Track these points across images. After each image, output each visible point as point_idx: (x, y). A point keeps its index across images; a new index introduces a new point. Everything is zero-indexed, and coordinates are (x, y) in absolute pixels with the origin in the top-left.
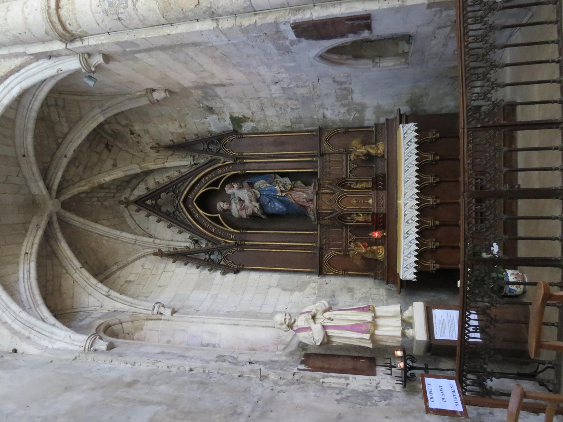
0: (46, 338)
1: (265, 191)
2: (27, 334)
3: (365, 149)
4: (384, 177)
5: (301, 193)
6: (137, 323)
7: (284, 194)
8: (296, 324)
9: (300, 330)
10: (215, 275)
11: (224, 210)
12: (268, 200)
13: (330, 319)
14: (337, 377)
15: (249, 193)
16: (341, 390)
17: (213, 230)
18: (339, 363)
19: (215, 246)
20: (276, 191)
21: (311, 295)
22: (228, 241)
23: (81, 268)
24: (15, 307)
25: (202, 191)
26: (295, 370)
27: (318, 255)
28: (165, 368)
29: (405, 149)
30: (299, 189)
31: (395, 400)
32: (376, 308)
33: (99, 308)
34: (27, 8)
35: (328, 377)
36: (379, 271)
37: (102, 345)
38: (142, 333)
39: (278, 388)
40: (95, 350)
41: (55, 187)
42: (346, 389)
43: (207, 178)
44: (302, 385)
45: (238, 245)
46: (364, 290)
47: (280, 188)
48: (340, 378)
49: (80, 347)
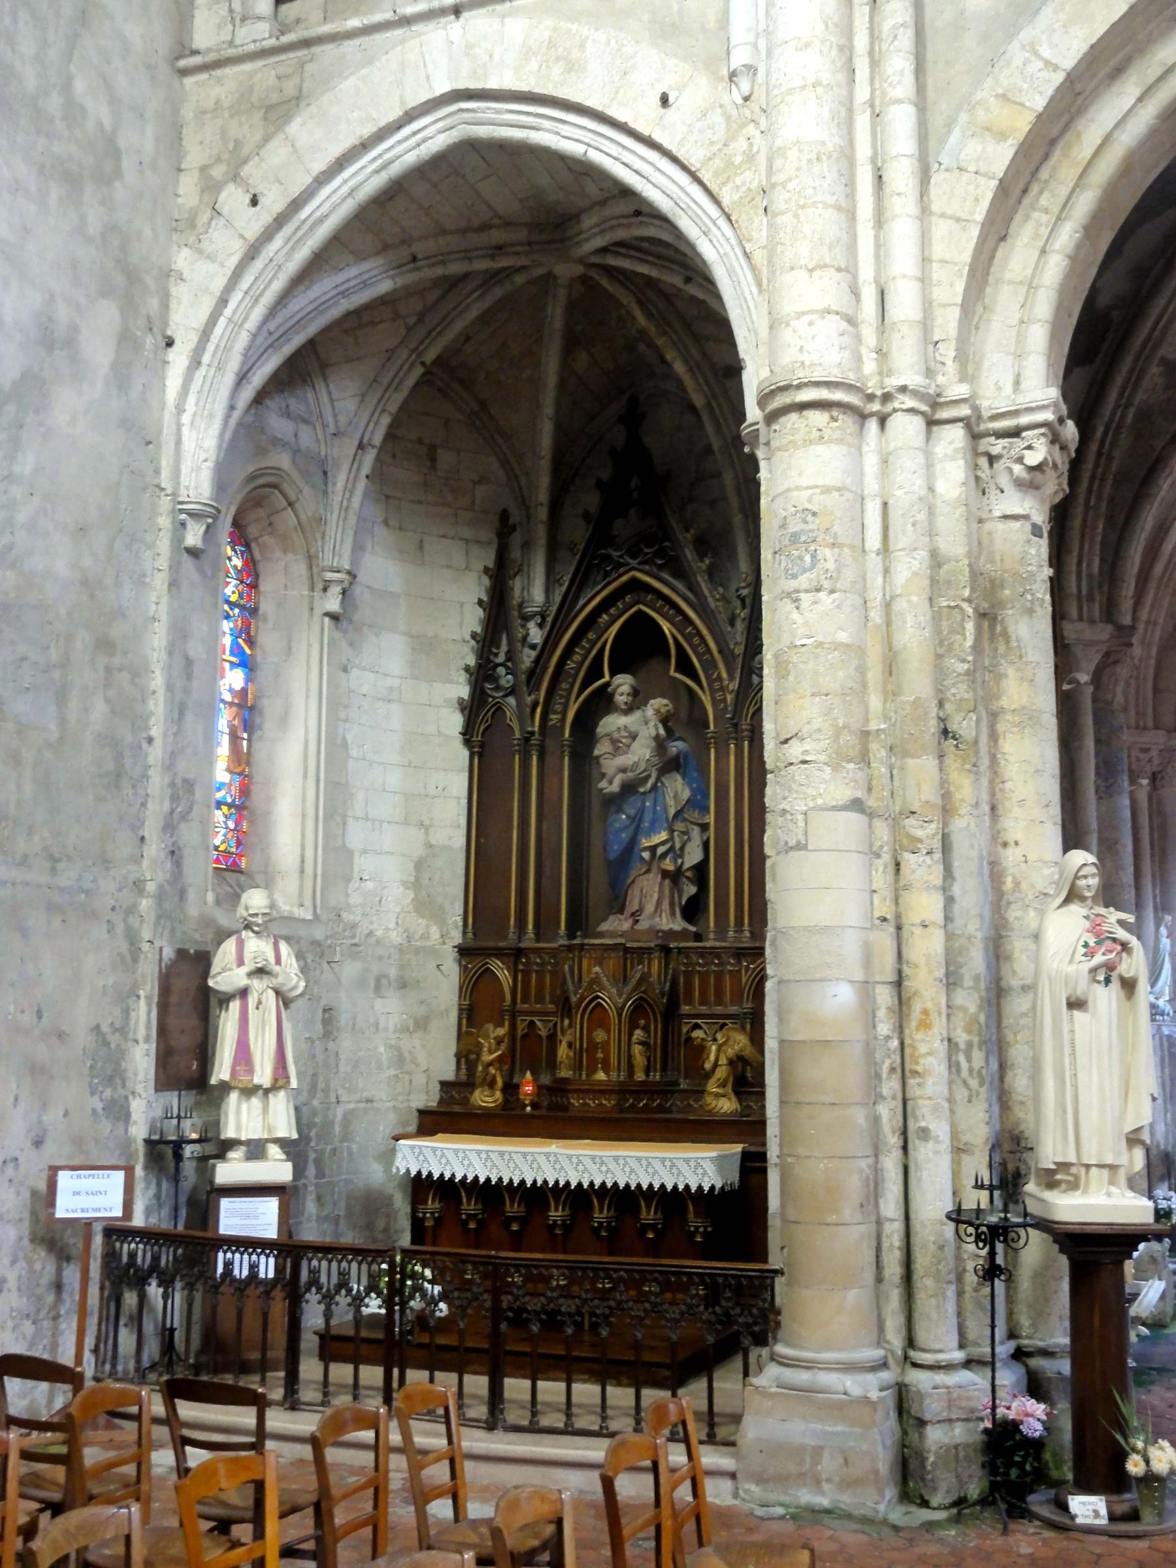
0: (201, 404)
1: (655, 806)
2: (206, 359)
3: (716, 1065)
4: (661, 1109)
5: (656, 896)
6: (298, 540)
7: (646, 855)
8: (251, 934)
9: (241, 944)
10: (458, 683)
11: (612, 695)
12: (632, 812)
13: (260, 1003)
14: (149, 1021)
15: (643, 766)
16: (123, 1030)
17: (570, 665)
18: (184, 1023)
19: (524, 677)
20: (652, 830)
21: (406, 931)
22: (539, 710)
23: (423, 364)
24: (277, 286)
25: (666, 627)
26: (157, 944)
27: (502, 944)
28: (152, 687)
29: (663, 1160)
30: (667, 891)
31: (106, 1126)
32: (282, 1094)
33: (332, 429)
34: (810, 324)
35: (149, 1005)
36: (459, 1093)
37: (194, 536)
38: (278, 554)
39: (117, 919)
40: (183, 524)
41: (612, 261)
42: (126, 1039)
43: (696, 640)
44: (128, 958)
45: (527, 740)
46: (422, 1057)
47: (663, 843)
48: (148, 1027)
49: (187, 488)
